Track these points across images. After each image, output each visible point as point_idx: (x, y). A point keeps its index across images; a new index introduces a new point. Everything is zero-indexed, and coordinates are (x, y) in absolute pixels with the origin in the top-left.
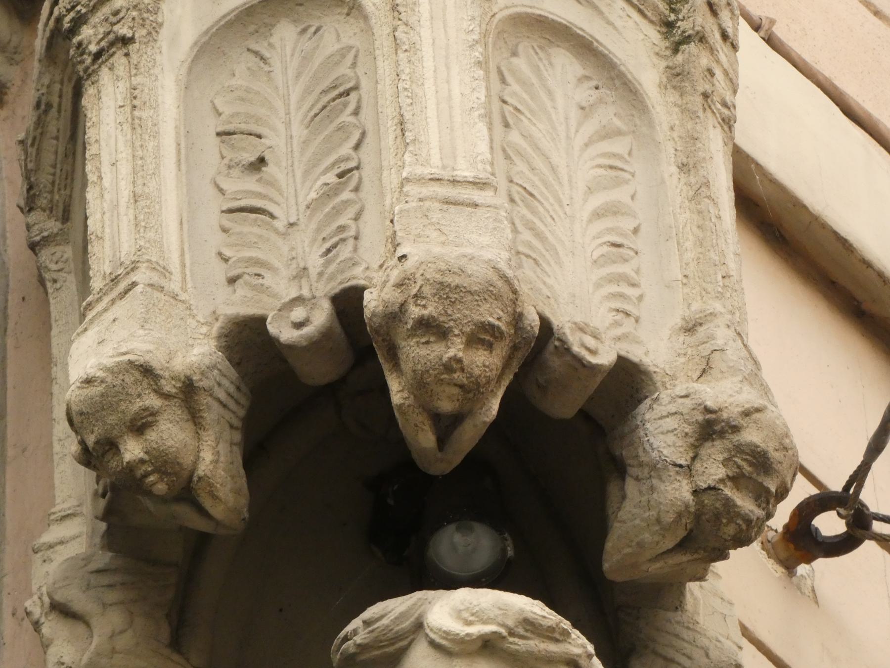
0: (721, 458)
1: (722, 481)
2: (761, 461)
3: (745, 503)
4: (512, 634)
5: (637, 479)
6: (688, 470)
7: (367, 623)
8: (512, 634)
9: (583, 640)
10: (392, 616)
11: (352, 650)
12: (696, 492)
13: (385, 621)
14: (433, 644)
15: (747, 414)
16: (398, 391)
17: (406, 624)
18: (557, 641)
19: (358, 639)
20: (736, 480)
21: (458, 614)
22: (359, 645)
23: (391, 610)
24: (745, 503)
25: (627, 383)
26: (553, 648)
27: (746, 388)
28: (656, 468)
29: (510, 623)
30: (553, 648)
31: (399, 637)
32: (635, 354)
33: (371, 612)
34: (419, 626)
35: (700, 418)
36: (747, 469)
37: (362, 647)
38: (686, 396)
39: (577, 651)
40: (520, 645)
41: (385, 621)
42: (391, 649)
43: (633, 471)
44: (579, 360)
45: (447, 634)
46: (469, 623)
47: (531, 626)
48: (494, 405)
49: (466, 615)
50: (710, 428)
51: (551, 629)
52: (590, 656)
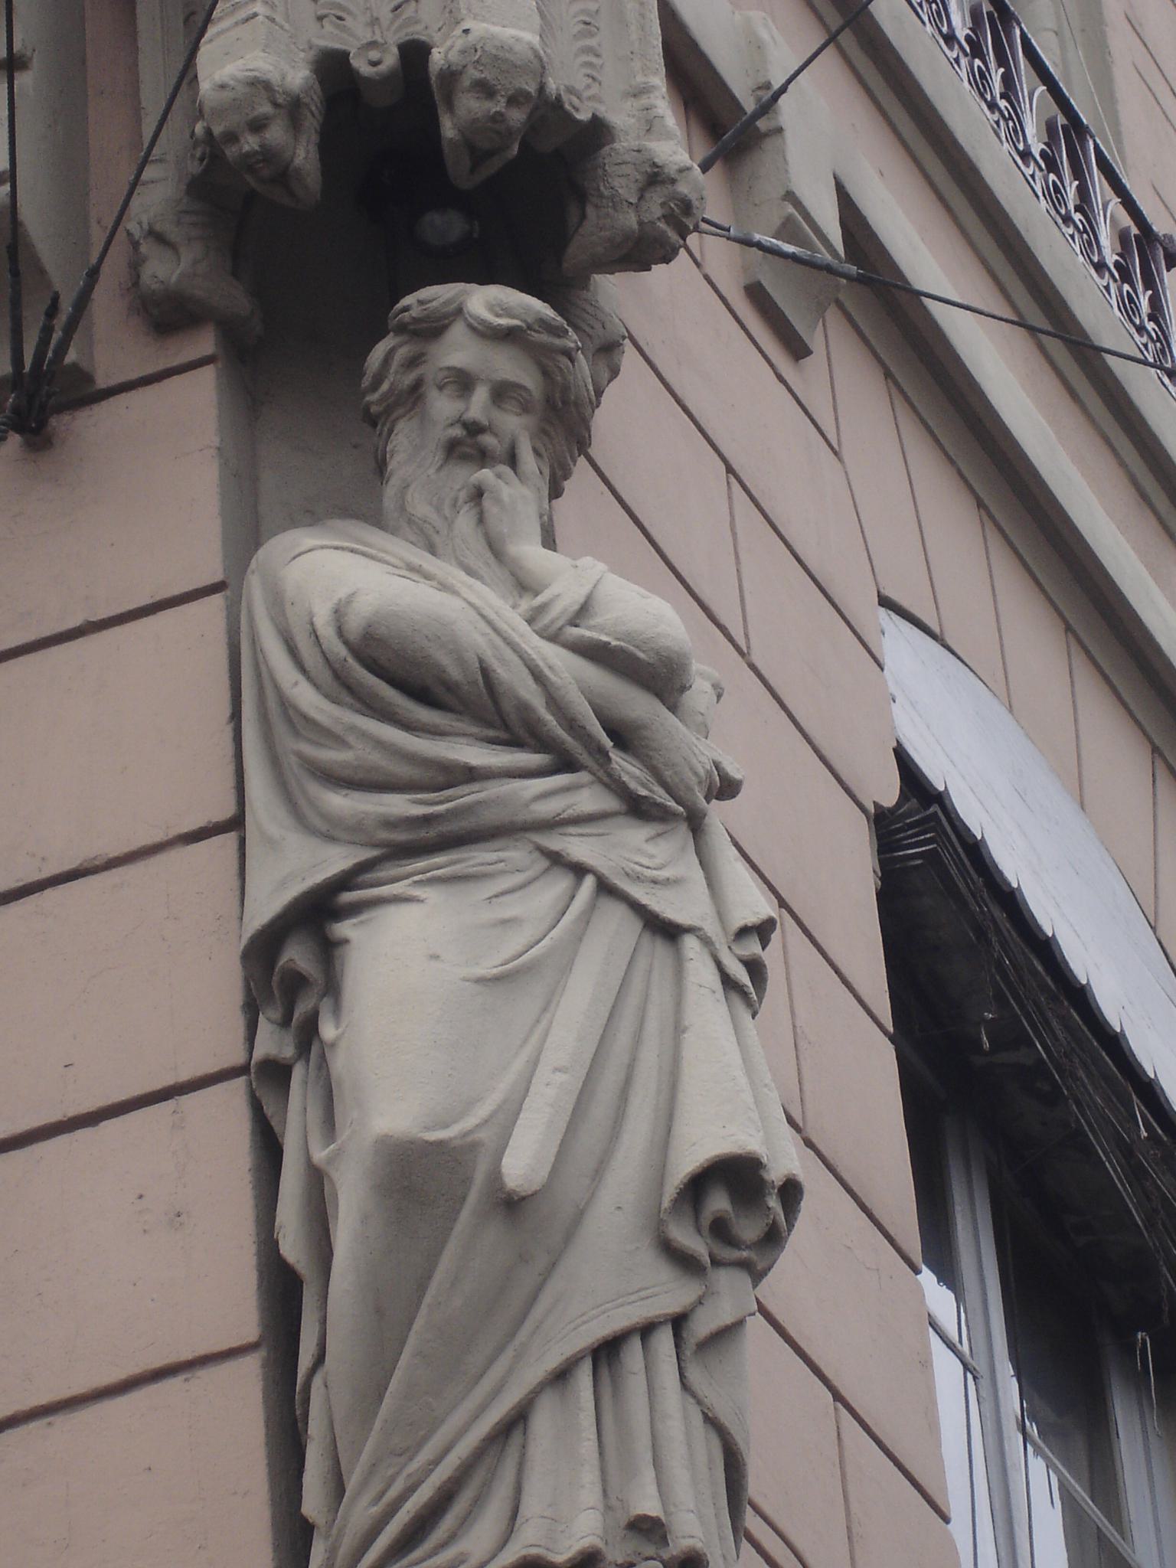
2: (687, 207)
4: (529, 327)
5: (597, 206)
6: (637, 207)
7: (421, 302)
10: (441, 300)
11: (407, 320)
12: (641, 223)
13: (434, 304)
15: (681, 171)
16: (448, 129)
18: (559, 337)
20: (669, 218)
21: (491, 308)
23: (438, 294)
24: (673, 236)
25: (598, 132)
26: (557, 342)
28: (616, 202)
30: (557, 342)
31: (445, 316)
32: (603, 111)
34: (459, 311)
37: (415, 320)
38: (639, 151)
39: (572, 345)
41: (434, 304)
43: (594, 200)
45: (483, 322)
46: (498, 316)
48: (515, 149)
49: (497, 309)
51: (557, 328)
52: (578, 349)
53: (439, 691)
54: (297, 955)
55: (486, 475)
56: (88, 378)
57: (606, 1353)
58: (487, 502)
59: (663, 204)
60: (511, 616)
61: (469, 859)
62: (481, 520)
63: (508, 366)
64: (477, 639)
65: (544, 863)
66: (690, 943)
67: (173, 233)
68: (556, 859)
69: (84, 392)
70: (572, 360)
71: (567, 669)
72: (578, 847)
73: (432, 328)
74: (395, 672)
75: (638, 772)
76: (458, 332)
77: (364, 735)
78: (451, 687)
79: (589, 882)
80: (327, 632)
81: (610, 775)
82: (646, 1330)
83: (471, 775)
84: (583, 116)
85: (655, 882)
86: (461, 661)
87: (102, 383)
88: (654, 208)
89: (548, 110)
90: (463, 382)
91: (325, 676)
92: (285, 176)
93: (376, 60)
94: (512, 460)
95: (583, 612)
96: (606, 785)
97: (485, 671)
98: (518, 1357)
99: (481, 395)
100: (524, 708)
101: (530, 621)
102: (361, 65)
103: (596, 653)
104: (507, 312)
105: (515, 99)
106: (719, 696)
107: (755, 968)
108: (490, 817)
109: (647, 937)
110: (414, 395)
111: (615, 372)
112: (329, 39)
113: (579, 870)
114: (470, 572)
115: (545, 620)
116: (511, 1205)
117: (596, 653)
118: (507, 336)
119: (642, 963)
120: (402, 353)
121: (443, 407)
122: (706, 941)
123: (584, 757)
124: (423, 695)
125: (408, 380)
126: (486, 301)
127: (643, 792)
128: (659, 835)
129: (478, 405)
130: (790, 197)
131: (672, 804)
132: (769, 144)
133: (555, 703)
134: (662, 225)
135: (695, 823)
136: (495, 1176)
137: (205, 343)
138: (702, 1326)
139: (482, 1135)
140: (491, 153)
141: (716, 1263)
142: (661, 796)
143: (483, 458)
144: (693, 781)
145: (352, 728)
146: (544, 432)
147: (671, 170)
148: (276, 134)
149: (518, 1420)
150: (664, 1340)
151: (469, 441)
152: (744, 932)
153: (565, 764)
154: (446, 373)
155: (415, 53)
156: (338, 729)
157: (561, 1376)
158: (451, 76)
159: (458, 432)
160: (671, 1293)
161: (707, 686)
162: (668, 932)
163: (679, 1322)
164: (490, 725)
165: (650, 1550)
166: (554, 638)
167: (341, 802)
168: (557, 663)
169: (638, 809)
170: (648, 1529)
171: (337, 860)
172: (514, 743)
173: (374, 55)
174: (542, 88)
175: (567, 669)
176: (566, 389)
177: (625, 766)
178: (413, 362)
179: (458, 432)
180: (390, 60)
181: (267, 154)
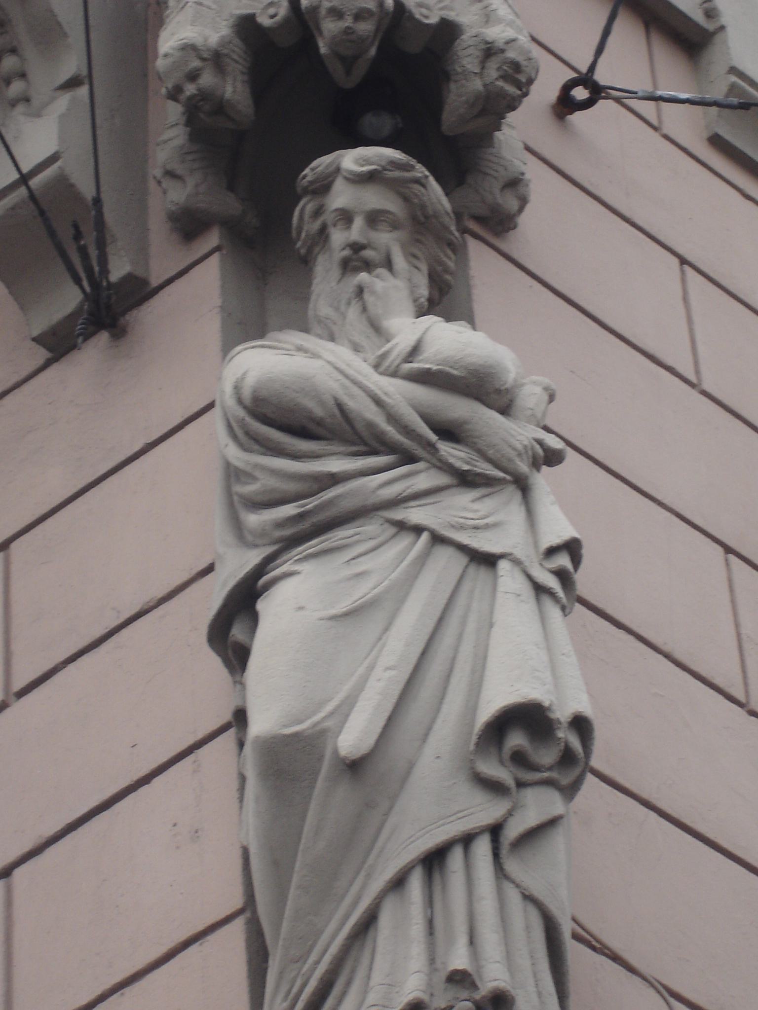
0: (496, 66)
1: (497, 79)
2: (516, 66)
3: (511, 89)
6: (480, 75)
7: (312, 170)
8: (386, 170)
9: (424, 169)
11: (306, 184)
12: (485, 85)
14: (347, 179)
15: (507, 43)
17: (331, 169)
18: (409, 171)
19: (309, 179)
20: (505, 77)
22: (309, 182)
23: (323, 162)
24: (511, 89)
25: (448, 31)
26: (407, 175)
27: (508, 29)
29: (383, 163)
30: (407, 175)
32: (451, 15)
33: (314, 164)
34: (338, 170)
35: (484, 47)
36: (510, 71)
37: (311, 183)
39: (420, 175)
40: (390, 174)
42: (325, 182)
44: (419, 22)
46: (362, 166)
47: (395, 164)
48: (373, 51)
50: (489, 51)
53: (312, 427)
54: (237, 633)
55: (363, 276)
56: (145, 282)
57: (434, 861)
58: (366, 296)
59: (499, 69)
60: (361, 367)
61: (334, 537)
62: (364, 309)
63: (374, 198)
64: (330, 384)
65: (392, 530)
66: (504, 566)
67: (180, 169)
68: (402, 526)
69: (139, 291)
70: (424, 186)
72: (415, 515)
73: (323, 187)
74: (280, 420)
75: (462, 454)
76: (339, 185)
77: (263, 468)
78: (319, 422)
79: (425, 536)
81: (440, 460)
82: (467, 840)
83: (334, 479)
84: (433, 20)
85: (476, 528)
86: (322, 403)
87: (155, 282)
88: (492, 73)
90: (346, 217)
92: (221, 108)
94: (388, 264)
95: (415, 351)
96: (440, 468)
97: (340, 406)
98: (369, 876)
99: (358, 223)
101: (376, 367)
102: (264, 21)
103: (425, 378)
104: (367, 161)
106: (551, 398)
107: (562, 575)
108: (348, 505)
111: (523, 201)
113: (418, 530)
115: (386, 363)
116: (355, 767)
117: (425, 378)
119: (466, 586)
120: (310, 208)
121: (338, 238)
122: (517, 562)
123: (419, 451)
124: (303, 433)
125: (316, 225)
126: (351, 159)
127: (466, 467)
128: (484, 496)
129: (357, 231)
130: (733, 70)
131: (501, 475)
132: (718, 38)
133: (393, 418)
134: (500, 83)
135: (523, 486)
136: (336, 751)
137: (213, 238)
138: (512, 831)
139: (328, 724)
140: (356, 58)
143: (368, 266)
144: (512, 454)
145: (256, 466)
146: (418, 241)
147: (500, 44)
148: (207, 79)
149: (369, 921)
150: (482, 847)
151: (354, 257)
152: (551, 552)
153: (409, 458)
154: (334, 214)
156: (248, 469)
157: (399, 883)
159: (347, 252)
160: (485, 810)
161: (538, 390)
162: (489, 561)
163: (495, 831)
164: (353, 444)
165: (465, 994)
167: (253, 519)
168: (391, 389)
169: (466, 480)
170: (459, 979)
171: (254, 558)
172: (374, 452)
173: (272, 11)
176: (423, 207)
179: (347, 252)
181: (204, 96)
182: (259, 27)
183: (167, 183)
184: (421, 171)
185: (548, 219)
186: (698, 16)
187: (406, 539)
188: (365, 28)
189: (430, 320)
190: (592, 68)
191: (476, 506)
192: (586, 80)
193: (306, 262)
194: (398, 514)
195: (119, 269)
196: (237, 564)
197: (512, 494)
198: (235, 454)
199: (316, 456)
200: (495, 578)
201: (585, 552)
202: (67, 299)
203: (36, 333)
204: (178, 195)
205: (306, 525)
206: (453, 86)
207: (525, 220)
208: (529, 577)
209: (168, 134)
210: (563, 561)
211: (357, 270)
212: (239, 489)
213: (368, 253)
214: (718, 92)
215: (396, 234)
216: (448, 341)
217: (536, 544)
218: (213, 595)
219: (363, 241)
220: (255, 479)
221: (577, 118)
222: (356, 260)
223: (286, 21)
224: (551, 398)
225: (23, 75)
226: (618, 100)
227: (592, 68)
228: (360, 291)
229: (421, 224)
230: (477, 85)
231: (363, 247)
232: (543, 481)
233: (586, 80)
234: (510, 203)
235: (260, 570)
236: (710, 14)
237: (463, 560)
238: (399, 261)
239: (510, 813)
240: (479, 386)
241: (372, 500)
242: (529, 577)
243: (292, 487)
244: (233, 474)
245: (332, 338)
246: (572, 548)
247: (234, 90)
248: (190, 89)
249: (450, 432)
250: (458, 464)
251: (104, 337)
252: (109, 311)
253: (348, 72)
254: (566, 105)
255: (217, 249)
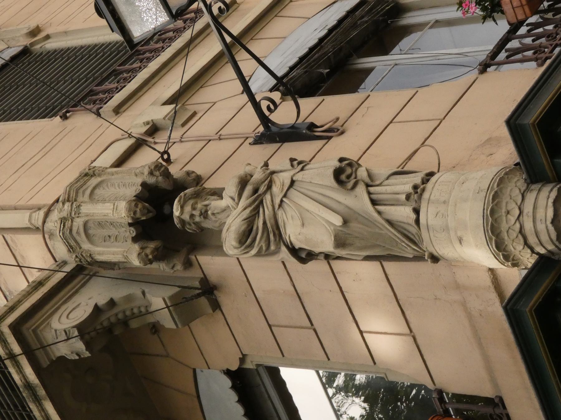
3: (163, 169)
6: (157, 177)
16: (144, 218)
20: (159, 170)
21: (177, 211)
23: (176, 221)
24: (163, 169)
28: (157, 181)
32: (140, 184)
33: (176, 223)
34: (178, 217)
40: (182, 202)
47: (179, 201)
48: (146, 204)
50: (151, 173)
53: (250, 228)
54: (303, 255)
55: (209, 212)
56: (202, 278)
57: (374, 203)
60: (235, 213)
63: (188, 208)
64: (239, 221)
66: (294, 179)
67: (171, 265)
68: (280, 206)
69: (204, 281)
71: (244, 202)
72: (277, 201)
73: (183, 222)
74: (246, 237)
76: (183, 217)
77: (259, 243)
78: (249, 225)
79: (284, 199)
80: (240, 249)
82: (369, 193)
83: (265, 223)
84: (140, 188)
86: (243, 224)
87: (202, 276)
88: (157, 173)
89: (139, 198)
90: (192, 216)
91: (249, 249)
92: (156, 249)
93: (132, 232)
95: (233, 199)
97: (245, 220)
98: (376, 221)
99: (194, 212)
100: (251, 211)
102: (134, 234)
103: (240, 195)
105: (136, 206)
106: (250, 164)
107: (300, 163)
108: (273, 221)
109: (294, 187)
110: (196, 224)
111: (193, 172)
112: (130, 241)
113: (282, 201)
114: (228, 216)
115: (234, 206)
116: (345, 222)
117: (240, 195)
118: (182, 207)
120: (188, 226)
121: (197, 219)
122: (294, 175)
123: (260, 198)
124: (250, 231)
125: (193, 225)
126: (176, 212)
129: (196, 213)
130: (164, 118)
132: (155, 122)
133: (250, 205)
135: (273, 173)
136: (340, 226)
137: (193, 257)
138: (368, 180)
139: (332, 228)
141: (356, 178)
142: (266, 182)
143: (206, 211)
144: (264, 175)
145: (258, 245)
148: (148, 251)
149: (389, 222)
150: (372, 189)
152: (292, 166)
153: (261, 202)
155: (130, 225)
156: (259, 247)
157: (379, 213)
158: (133, 218)
159: (202, 217)
162: (293, 182)
163: (368, 186)
165: (412, 197)
166: (238, 204)
167: (273, 248)
168: (242, 205)
169: (269, 187)
170: (408, 197)
171: (284, 248)
172: (258, 212)
173: (132, 232)
174: (134, 200)
175: (244, 202)
176: (192, 195)
177: (262, 189)
178: (190, 225)
179: (202, 217)
180: (132, 229)
181: (152, 253)
182: (136, 236)
183: (175, 269)
184: (182, 194)
185: (199, 167)
186: (148, 126)
187: (284, 205)
188: (140, 206)
189: (224, 194)
190: (159, 152)
191: (277, 185)
192: (162, 154)
193: (202, 229)
194: (277, 206)
195: (197, 284)
196: (284, 253)
197: (275, 176)
198: (254, 251)
199: (258, 228)
200: (297, 181)
201: (293, 157)
202: (203, 301)
203: (211, 311)
204: (179, 267)
205: (277, 232)
206: (159, 185)
207: (199, 172)
208: (298, 172)
209: (161, 267)
210: (295, 163)
211: (207, 214)
212: (263, 253)
213: (203, 211)
214: (170, 123)
215: (199, 202)
216: (231, 190)
217: (290, 170)
218: (292, 262)
219: (199, 212)
220: (262, 246)
221: (172, 158)
222: (204, 214)
223: (135, 228)
224: (250, 164)
225: (139, 307)
226: (168, 148)
227: (159, 152)
228: (213, 214)
229: (197, 195)
230: (160, 178)
231: (201, 212)
232: (272, 167)
233: (162, 154)
234: (193, 175)
235: (287, 246)
236: (148, 123)
237: (291, 189)
238: (206, 203)
239: (363, 181)
240: (243, 182)
241: (272, 213)
242: (298, 172)
243: (265, 235)
244: (259, 254)
245: (225, 223)
246: (292, 160)
247: (152, 245)
248: (150, 257)
249: (256, 191)
250: (265, 189)
251: (215, 292)
252: (209, 289)
253: (151, 212)
254: (168, 161)
255: (196, 257)
